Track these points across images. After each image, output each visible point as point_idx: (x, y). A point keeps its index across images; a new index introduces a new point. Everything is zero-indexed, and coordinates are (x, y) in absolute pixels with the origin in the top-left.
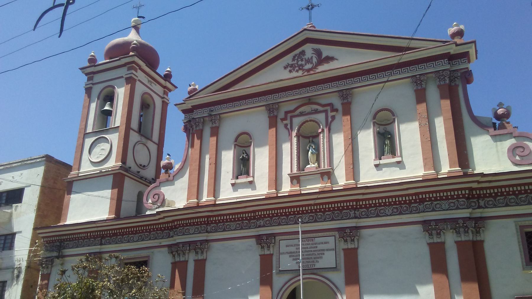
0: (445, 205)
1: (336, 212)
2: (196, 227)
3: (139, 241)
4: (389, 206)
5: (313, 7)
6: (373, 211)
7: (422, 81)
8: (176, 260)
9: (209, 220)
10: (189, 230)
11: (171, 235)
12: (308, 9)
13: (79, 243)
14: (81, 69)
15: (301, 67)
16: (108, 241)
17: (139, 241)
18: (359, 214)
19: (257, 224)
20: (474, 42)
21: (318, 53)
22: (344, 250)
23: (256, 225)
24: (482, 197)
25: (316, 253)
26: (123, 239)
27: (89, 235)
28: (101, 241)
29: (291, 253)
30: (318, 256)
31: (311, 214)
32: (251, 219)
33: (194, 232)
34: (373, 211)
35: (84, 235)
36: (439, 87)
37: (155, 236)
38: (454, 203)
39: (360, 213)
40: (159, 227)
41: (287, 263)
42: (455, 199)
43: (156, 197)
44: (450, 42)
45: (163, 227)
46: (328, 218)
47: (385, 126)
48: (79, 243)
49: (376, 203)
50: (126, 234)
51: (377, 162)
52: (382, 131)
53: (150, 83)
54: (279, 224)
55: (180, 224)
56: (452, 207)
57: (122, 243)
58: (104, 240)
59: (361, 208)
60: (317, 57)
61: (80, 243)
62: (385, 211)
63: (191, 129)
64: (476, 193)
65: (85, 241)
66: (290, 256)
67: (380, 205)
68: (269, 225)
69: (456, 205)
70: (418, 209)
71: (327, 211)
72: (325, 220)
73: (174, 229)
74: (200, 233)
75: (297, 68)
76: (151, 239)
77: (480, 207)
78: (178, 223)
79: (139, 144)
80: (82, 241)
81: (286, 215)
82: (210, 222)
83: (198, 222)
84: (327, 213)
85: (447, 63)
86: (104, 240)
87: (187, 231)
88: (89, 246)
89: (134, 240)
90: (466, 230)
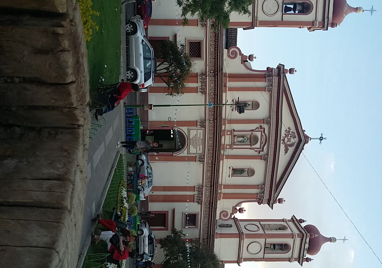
8: (198, 77)
11: (211, 72)
20: (272, 209)
21: (291, 145)
22: (196, 156)
25: (196, 146)
29: (197, 135)
36: (257, 194)
41: (193, 133)
45: (216, 67)
47: (247, 171)
50: (215, 43)
51: (231, 168)
52: (245, 170)
66: (195, 135)
67: (212, 172)
73: (214, 74)
74: (210, 90)
77: (206, 203)
87: (212, 82)
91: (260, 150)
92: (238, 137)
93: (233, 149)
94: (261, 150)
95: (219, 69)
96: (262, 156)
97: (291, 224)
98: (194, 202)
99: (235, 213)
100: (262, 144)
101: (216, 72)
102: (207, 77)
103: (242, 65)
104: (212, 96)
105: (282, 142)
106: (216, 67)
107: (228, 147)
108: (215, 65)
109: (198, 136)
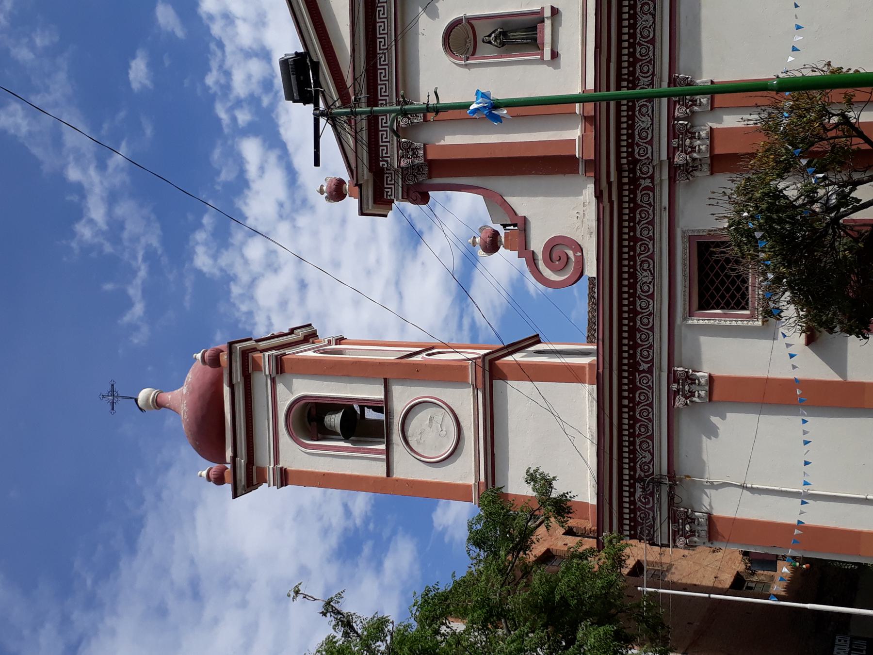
3: (652, 269)
10: (641, 131)
11: (647, 183)
13: (641, 435)
16: (645, 353)
17: (652, 269)
26: (643, 311)
28: (644, 371)
35: (626, 416)
37: (647, 225)
45: (629, 202)
50: (634, 303)
55: (627, 152)
58: (642, 363)
61: (643, 430)
65: (638, 416)
76: (652, 234)
86: (642, 363)
87: (644, 134)
88: (651, 405)
89: (650, 283)
101: (629, 184)
102: (669, 158)
106: (629, 202)
108: (633, 211)
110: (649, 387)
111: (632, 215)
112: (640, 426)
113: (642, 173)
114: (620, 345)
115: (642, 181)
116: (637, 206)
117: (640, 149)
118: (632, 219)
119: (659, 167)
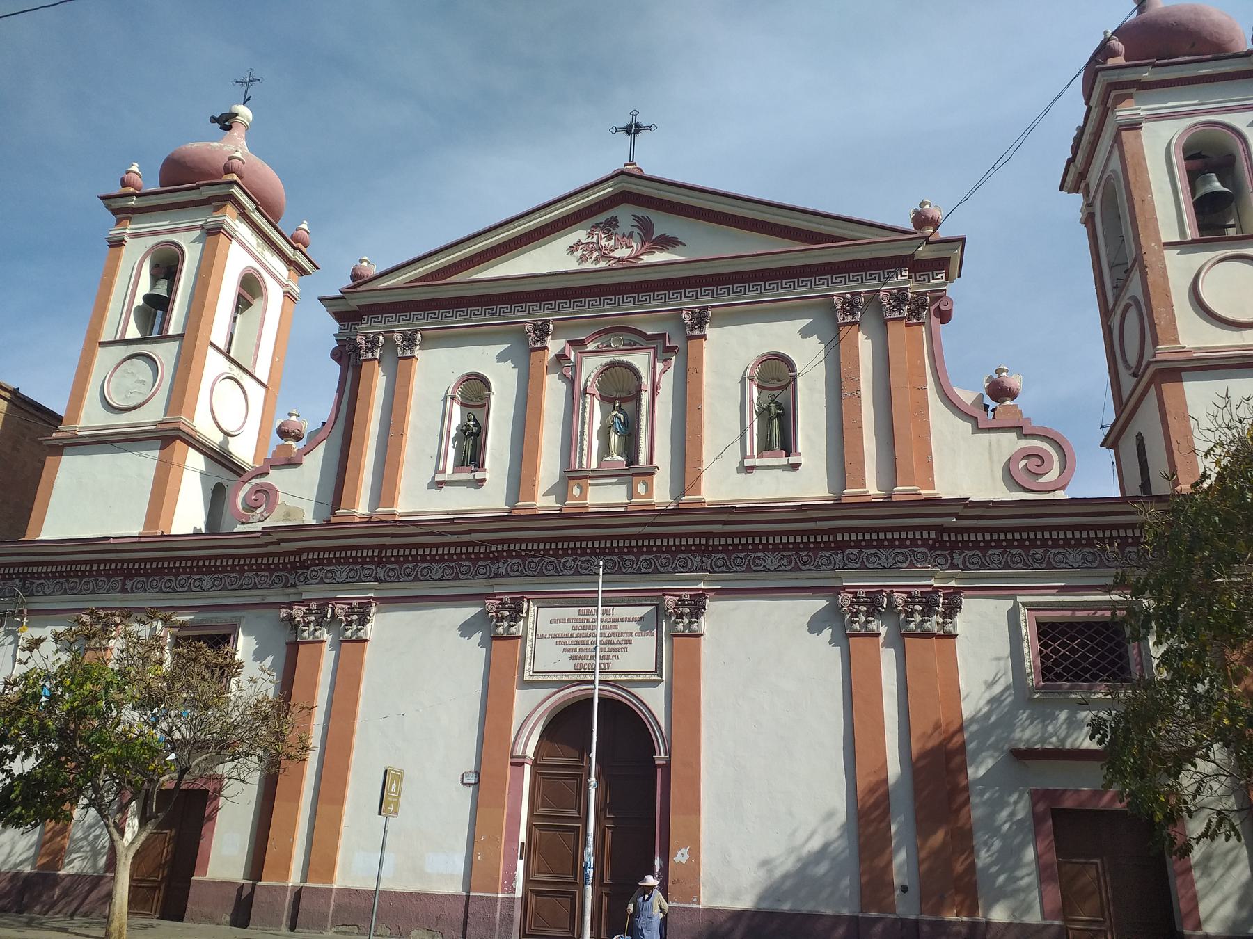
0: (887, 557)
1: (663, 556)
2: (351, 567)
4: (773, 550)
5: (639, 128)
6: (739, 560)
7: (855, 307)
9: (383, 555)
11: (291, 581)
12: (629, 132)
13: (68, 584)
14: (102, 198)
15: (606, 252)
16: (139, 585)
18: (711, 563)
19: (491, 570)
20: (962, 240)
21: (645, 228)
23: (489, 571)
24: (959, 548)
25: (615, 639)
26: (177, 582)
27: (96, 569)
28: (124, 584)
30: (618, 646)
31: (609, 557)
32: (478, 559)
33: (347, 578)
34: (739, 560)
35: (83, 569)
37: (253, 582)
38: (904, 555)
39: (713, 562)
40: (265, 562)
42: (907, 547)
43: (259, 494)
44: (916, 233)
45: (273, 563)
46: (646, 568)
48: (68, 584)
49: (747, 544)
50: (186, 573)
53: (261, 250)
54: (541, 574)
55: (314, 559)
56: (900, 562)
57: (174, 590)
58: (132, 582)
59: (718, 552)
60: (641, 233)
61: (72, 585)
62: (765, 562)
63: (353, 356)
64: (950, 540)
65: (84, 580)
66: (558, 644)
67: (756, 549)
68: (517, 573)
69: (909, 559)
70: (833, 562)
71: (647, 553)
72: (638, 572)
73: (300, 568)
74: (360, 580)
75: (596, 254)
77: (953, 567)
78: (310, 557)
79: (225, 378)
80: (77, 580)
81: (556, 553)
82: (384, 559)
83: (357, 557)
84: (643, 557)
85: (906, 276)
86: (132, 582)
87: (329, 575)
88: (93, 592)
90: (926, 611)
91: (660, 350)
92: (609, 454)
93: (656, 462)
94: (659, 344)
95: (269, 547)
96: (690, 333)
97: (1094, 177)
98: (955, 636)
99: (1020, 412)
100: (635, 344)
103: (303, 462)
104: (391, 573)
105: (627, 264)
107: (641, 489)
109: (566, 628)
110: (109, 589)
111: (263, 567)
112: (76, 582)
113: (299, 576)
114: (145, 560)
115: (293, 576)
116: (271, 571)
117: (317, 571)
118: (259, 566)
119: (296, 592)
